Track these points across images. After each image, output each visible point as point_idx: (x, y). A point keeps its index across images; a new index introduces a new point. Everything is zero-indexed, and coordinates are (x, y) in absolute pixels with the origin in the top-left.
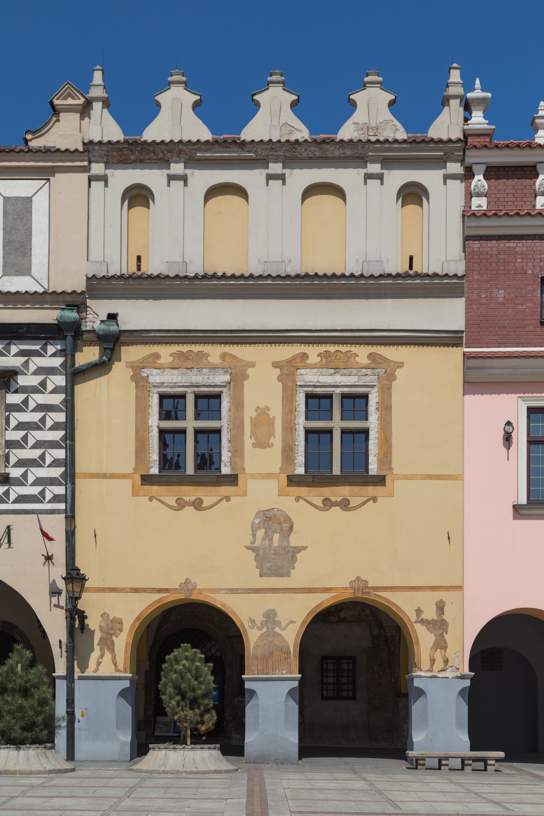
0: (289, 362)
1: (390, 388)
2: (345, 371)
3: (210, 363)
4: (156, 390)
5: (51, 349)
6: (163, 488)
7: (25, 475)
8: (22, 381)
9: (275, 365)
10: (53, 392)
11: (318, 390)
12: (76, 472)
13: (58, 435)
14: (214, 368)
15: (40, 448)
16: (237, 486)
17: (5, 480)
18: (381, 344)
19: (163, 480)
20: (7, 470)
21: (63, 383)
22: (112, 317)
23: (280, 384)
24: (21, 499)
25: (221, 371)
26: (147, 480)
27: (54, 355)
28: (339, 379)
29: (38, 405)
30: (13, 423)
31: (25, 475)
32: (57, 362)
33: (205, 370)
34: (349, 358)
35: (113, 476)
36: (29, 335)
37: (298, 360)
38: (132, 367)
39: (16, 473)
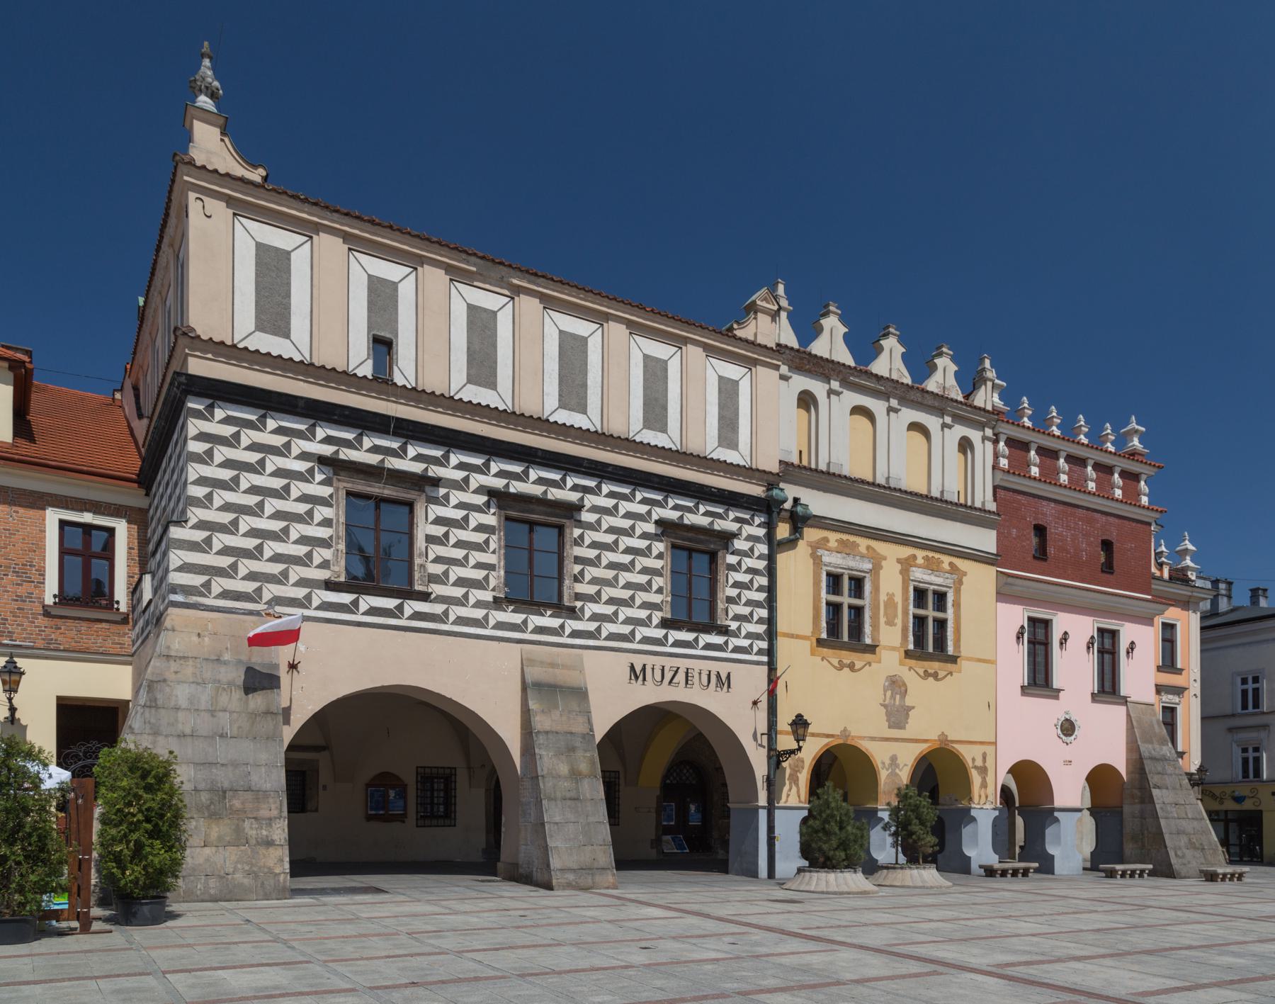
0: (907, 559)
1: (960, 590)
2: (937, 573)
3: (861, 553)
4: (825, 568)
5: (757, 520)
6: (830, 650)
7: (739, 628)
8: (739, 544)
9: (899, 561)
10: (758, 558)
11: (921, 585)
12: (779, 630)
13: (761, 596)
14: (862, 556)
15: (749, 606)
16: (875, 654)
17: (724, 631)
18: (955, 556)
19: (832, 644)
20: (728, 623)
21: (766, 552)
22: (796, 500)
23: (901, 577)
24: (737, 649)
25: (867, 560)
26: (820, 642)
27: (759, 526)
28: (933, 579)
29: (748, 568)
30: (731, 582)
31: (739, 628)
32: (761, 532)
33: (858, 558)
34: (939, 563)
35: (798, 637)
36: (745, 505)
37: (911, 559)
38: (811, 546)
39: (734, 625)
